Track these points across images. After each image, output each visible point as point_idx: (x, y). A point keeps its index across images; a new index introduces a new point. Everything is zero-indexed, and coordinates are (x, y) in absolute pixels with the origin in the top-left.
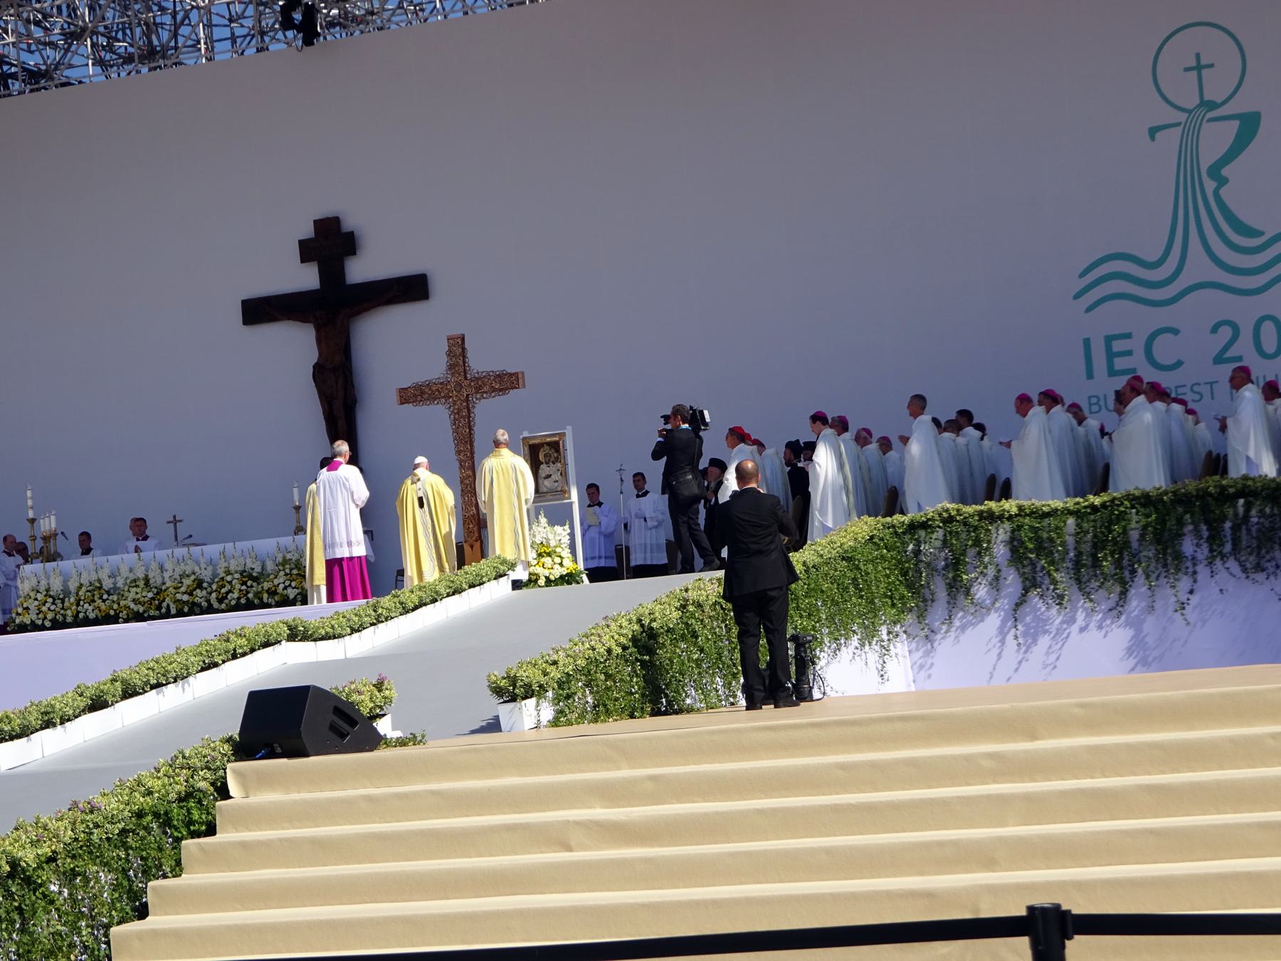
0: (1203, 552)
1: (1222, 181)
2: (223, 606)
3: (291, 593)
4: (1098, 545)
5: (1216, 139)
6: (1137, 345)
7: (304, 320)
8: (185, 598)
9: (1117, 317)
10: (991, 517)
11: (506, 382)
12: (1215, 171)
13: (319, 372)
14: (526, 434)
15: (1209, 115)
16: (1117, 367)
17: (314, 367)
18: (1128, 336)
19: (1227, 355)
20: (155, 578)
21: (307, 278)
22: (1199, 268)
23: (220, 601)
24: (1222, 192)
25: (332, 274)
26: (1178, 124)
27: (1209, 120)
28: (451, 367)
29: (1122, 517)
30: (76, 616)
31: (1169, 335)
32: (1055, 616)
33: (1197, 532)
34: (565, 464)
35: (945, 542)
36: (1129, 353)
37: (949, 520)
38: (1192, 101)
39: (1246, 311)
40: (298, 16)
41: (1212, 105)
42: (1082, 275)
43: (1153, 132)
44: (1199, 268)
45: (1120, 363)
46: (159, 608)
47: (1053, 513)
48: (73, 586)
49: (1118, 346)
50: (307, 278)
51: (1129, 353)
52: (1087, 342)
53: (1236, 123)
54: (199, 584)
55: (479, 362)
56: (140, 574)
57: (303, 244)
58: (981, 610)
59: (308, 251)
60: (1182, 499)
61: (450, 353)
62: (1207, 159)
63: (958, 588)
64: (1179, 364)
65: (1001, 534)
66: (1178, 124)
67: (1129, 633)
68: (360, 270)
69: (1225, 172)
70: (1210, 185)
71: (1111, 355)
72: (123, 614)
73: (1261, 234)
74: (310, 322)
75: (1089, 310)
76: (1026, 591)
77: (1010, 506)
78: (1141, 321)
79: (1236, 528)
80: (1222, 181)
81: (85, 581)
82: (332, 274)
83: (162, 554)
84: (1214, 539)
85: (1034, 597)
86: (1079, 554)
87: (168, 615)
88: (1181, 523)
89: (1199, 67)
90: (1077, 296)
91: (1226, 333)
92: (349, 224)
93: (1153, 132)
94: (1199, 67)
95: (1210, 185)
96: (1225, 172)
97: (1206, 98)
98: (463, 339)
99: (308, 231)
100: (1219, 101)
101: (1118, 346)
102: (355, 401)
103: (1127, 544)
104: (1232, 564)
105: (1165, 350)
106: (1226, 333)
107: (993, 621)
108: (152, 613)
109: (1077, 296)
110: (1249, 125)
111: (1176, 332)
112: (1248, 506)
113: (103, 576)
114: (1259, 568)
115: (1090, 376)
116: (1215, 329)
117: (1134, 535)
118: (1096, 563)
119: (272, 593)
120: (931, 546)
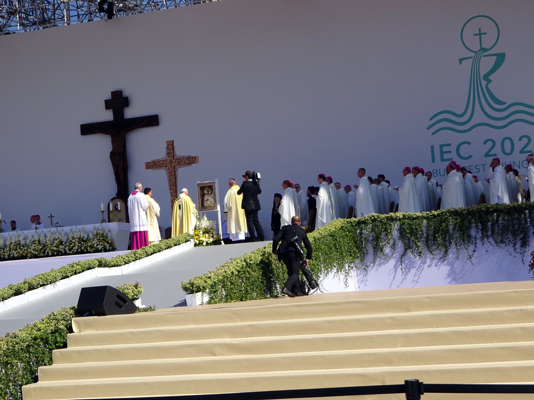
0: (479, 235)
1: (489, 81)
2: (71, 252)
3: (100, 247)
4: (436, 231)
5: (487, 64)
6: (453, 148)
7: (106, 133)
8: (55, 249)
9: (445, 137)
10: (392, 219)
11: (191, 160)
12: (486, 77)
13: (113, 155)
14: (199, 182)
15: (485, 54)
16: (445, 158)
17: (111, 153)
18: (449, 145)
19: (490, 153)
20: (43, 240)
21: (108, 116)
22: (479, 117)
23: (70, 250)
24: (489, 86)
25: (118, 113)
26: (471, 57)
27: (484, 56)
28: (168, 154)
29: (446, 220)
30: (9, 256)
31: (466, 145)
32: (418, 261)
33: (477, 226)
34: (215, 195)
35: (372, 229)
36: (450, 152)
37: (375, 220)
38: (477, 48)
39: (498, 135)
40: (105, 7)
41: (486, 50)
42: (430, 120)
43: (461, 61)
44: (479, 117)
45: (446, 156)
46: (44, 253)
47: (418, 218)
48: (8, 243)
49: (445, 149)
50: (108, 116)
51: (450, 152)
52: (432, 147)
53: (495, 57)
54: (61, 243)
55: (180, 152)
56: (36, 238)
57: (106, 102)
58: (387, 258)
59: (108, 105)
60: (470, 213)
61: (167, 148)
62: (483, 72)
63: (378, 249)
64: (470, 157)
65: (396, 226)
66: (471, 57)
67: (448, 268)
68: (130, 113)
69: (490, 77)
70: (484, 83)
71: (442, 153)
72: (29, 255)
73: (505, 103)
74: (109, 134)
75: (433, 134)
76: (406, 250)
77: (399, 214)
78: (454, 138)
79: (493, 225)
80: (489, 81)
81: (13, 241)
82: (118, 113)
83: (46, 230)
84: (484, 229)
85: (409, 252)
86: (428, 235)
87: (48, 256)
88: (470, 223)
89: (480, 34)
90: (429, 128)
91: (490, 144)
92: (126, 93)
93: (461, 61)
94: (480, 34)
95: (484, 83)
96: (490, 77)
97: (483, 47)
98: (173, 142)
99: (108, 96)
100: (488, 48)
101: (445, 149)
102: (127, 168)
103: (448, 231)
104: (491, 240)
105: (464, 151)
106: (490, 144)
107: (392, 262)
108: (41, 255)
109: (429, 128)
110: (501, 58)
111: (469, 143)
112: (498, 216)
113: (21, 238)
114: (502, 242)
115: (433, 161)
116: (485, 143)
117: (451, 227)
118: (435, 239)
119: (92, 247)
120: (367, 231)
